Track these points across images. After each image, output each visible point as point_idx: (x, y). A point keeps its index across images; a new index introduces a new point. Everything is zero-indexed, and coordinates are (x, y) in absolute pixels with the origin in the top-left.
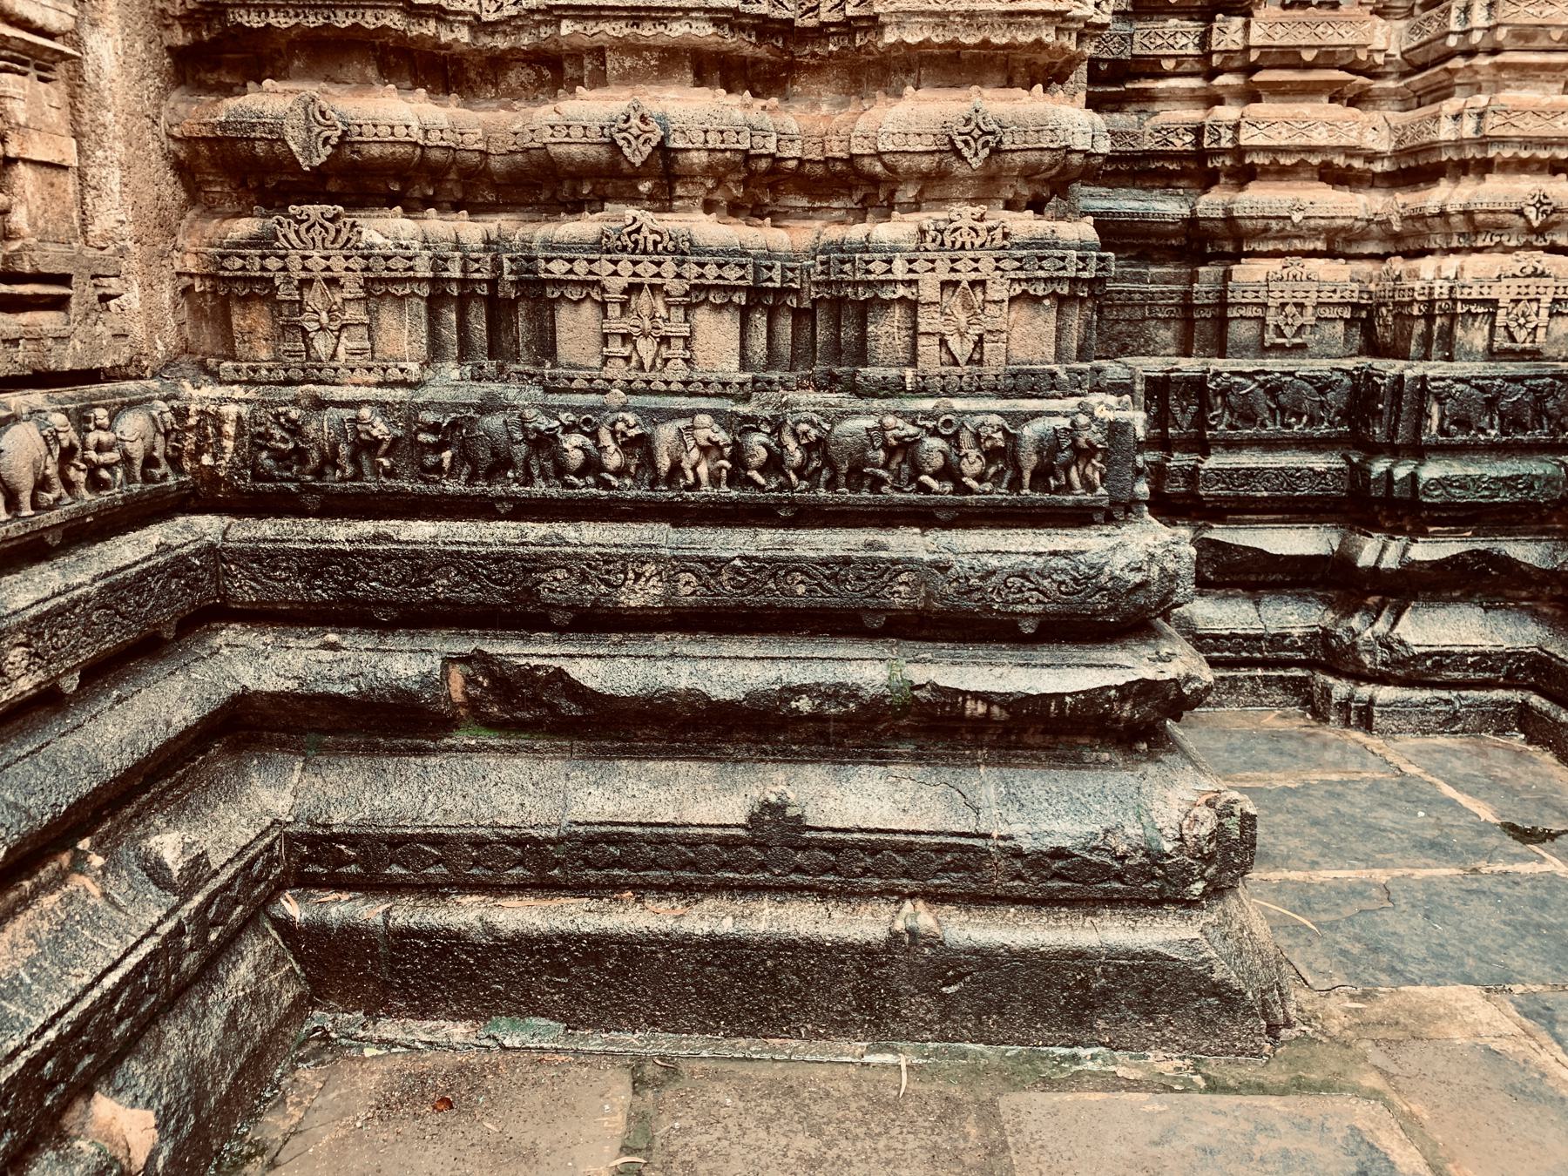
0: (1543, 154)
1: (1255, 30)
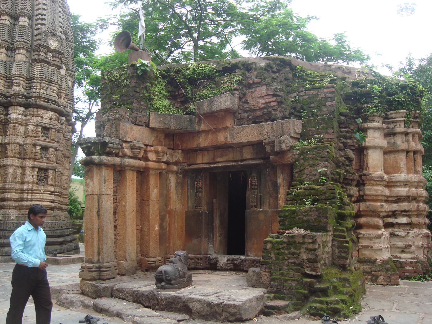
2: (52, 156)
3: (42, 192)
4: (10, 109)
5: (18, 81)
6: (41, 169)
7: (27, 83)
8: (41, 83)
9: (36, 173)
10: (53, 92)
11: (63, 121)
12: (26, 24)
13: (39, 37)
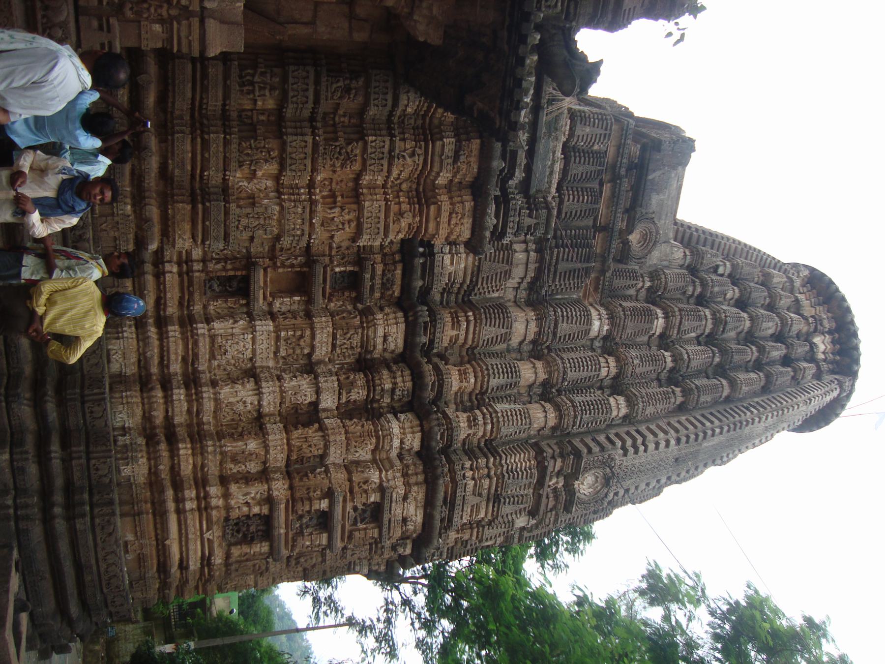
0: (165, 353)
1: (197, 274)
2: (308, 543)
3: (207, 536)
4: (409, 415)
5: (481, 422)
6: (267, 521)
7: (479, 443)
8: (489, 476)
9: (256, 510)
10: (472, 511)
11: (401, 550)
12: (614, 413)
13: (596, 449)
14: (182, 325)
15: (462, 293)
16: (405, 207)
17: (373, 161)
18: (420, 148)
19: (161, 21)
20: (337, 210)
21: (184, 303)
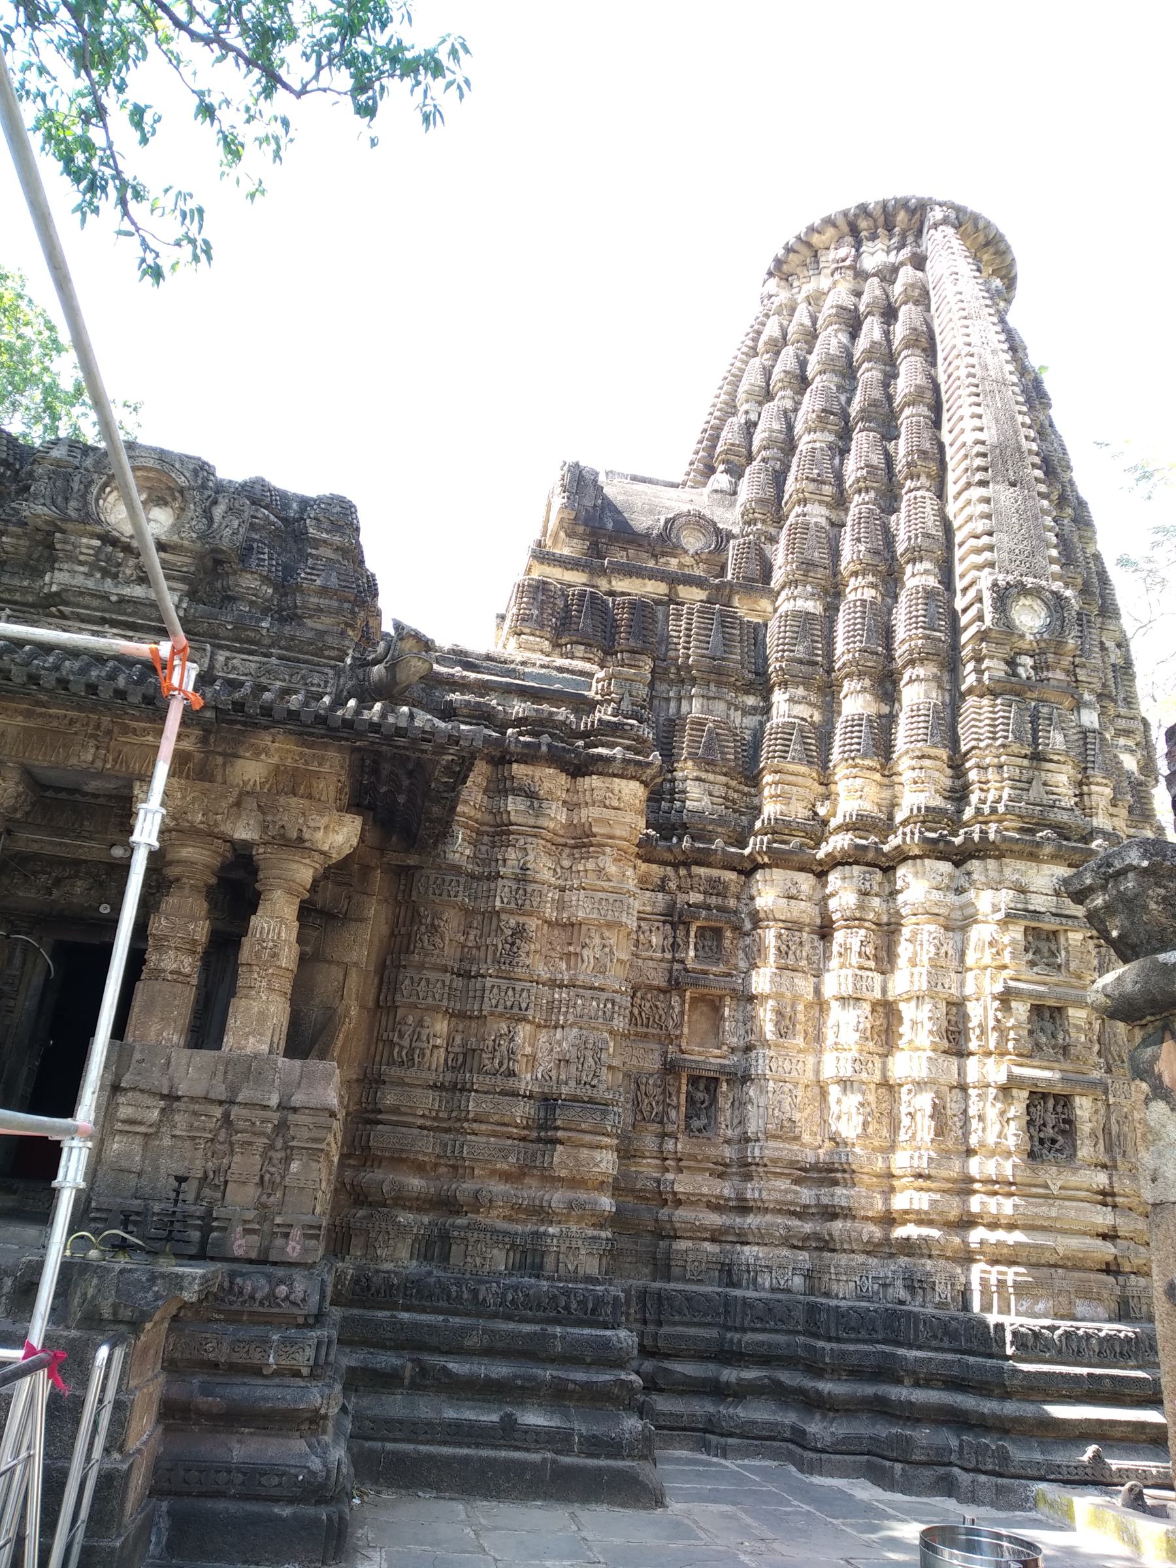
1: (679, 1146)
4: (901, 871)
6: (1038, 1096)
14: (748, 1177)
15: (742, 787)
16: (591, 865)
17: (528, 902)
18: (517, 840)
19: (288, 1160)
20: (585, 952)
21: (721, 1170)
